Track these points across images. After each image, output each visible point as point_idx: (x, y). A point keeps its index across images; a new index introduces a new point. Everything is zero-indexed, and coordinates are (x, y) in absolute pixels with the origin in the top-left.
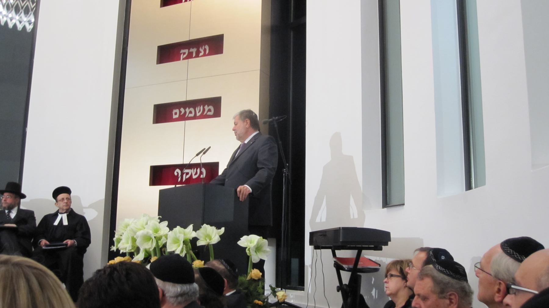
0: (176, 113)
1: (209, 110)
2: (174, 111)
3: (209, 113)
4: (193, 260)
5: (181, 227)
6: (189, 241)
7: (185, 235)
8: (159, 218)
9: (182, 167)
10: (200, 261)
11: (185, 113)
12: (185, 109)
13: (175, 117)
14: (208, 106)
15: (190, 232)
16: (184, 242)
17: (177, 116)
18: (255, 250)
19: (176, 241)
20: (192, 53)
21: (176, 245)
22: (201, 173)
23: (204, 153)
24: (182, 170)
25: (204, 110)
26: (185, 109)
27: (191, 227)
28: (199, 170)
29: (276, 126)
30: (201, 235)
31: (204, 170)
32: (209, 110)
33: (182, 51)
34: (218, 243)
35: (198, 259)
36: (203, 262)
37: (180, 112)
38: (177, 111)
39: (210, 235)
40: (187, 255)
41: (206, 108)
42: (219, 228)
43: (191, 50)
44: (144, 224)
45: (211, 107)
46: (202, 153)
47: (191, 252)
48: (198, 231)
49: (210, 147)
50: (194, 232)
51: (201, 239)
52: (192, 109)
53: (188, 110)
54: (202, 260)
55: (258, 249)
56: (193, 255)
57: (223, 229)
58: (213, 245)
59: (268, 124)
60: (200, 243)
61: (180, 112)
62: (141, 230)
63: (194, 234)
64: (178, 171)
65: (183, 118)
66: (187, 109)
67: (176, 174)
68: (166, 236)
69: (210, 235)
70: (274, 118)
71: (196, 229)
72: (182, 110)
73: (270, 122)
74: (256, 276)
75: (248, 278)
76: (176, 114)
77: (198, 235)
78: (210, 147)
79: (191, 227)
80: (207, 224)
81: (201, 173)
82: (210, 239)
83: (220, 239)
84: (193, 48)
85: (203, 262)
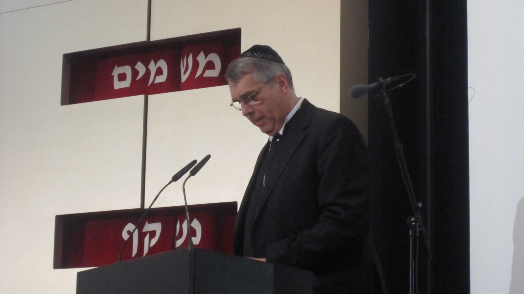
0: (122, 75)
1: (210, 65)
2: (117, 71)
3: (209, 73)
9: (140, 216)
12: (146, 64)
13: (118, 85)
14: (206, 56)
17: (126, 84)
22: (192, 232)
23: (193, 173)
24: (140, 227)
25: (196, 65)
26: (146, 64)
28: (185, 226)
29: (387, 101)
31: (196, 224)
32: (210, 65)
37: (135, 73)
38: (127, 70)
41: (202, 59)
45: (214, 58)
46: (188, 173)
49: (208, 157)
52: (163, 64)
59: (364, 99)
61: (135, 73)
64: (130, 227)
65: (142, 87)
67: (125, 236)
70: (381, 79)
72: (140, 67)
73: (372, 92)
76: (122, 77)
78: (208, 157)
81: (192, 232)
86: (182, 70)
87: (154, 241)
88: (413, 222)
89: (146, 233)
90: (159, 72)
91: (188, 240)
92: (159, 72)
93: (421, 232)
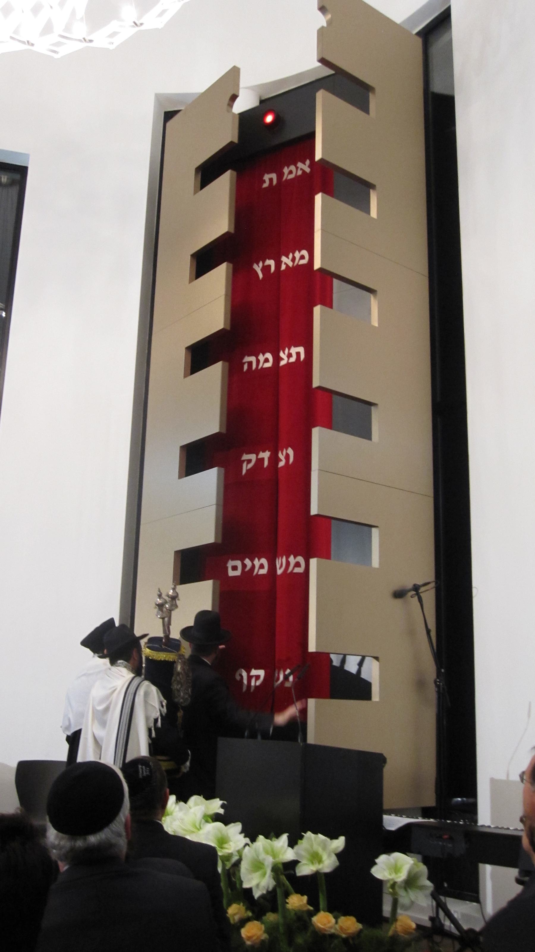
4: (287, 895)
5: (267, 837)
6: (281, 866)
7: (274, 856)
8: (223, 806)
11: (253, 566)
12: (252, 560)
15: (281, 849)
16: (275, 869)
18: (403, 885)
19: (258, 866)
20: (263, 459)
21: (257, 875)
26: (252, 560)
27: (284, 838)
30: (303, 853)
33: (245, 457)
34: (336, 872)
35: (297, 892)
36: (305, 898)
37: (244, 566)
38: (238, 563)
39: (320, 853)
40: (278, 890)
41: (292, 559)
42: (333, 836)
43: (261, 455)
44: (198, 827)
47: (283, 878)
48: (296, 847)
50: (290, 849)
51: (304, 862)
53: (257, 562)
54: (302, 895)
55: (410, 882)
56: (287, 883)
57: (342, 839)
58: (326, 874)
61: (244, 566)
62: (193, 832)
63: (289, 855)
66: (256, 559)
67: (238, 678)
68: (240, 852)
69: (320, 853)
71: (292, 843)
72: (248, 562)
75: (391, 933)
77: (297, 854)
79: (284, 838)
82: (320, 861)
83: (337, 863)
84: (264, 451)
85: (305, 898)
86: (278, 566)
87: (258, 683)
88: (438, 682)
89: (252, 676)
90: (262, 566)
91: (283, 683)
92: (262, 566)
93: (443, 689)
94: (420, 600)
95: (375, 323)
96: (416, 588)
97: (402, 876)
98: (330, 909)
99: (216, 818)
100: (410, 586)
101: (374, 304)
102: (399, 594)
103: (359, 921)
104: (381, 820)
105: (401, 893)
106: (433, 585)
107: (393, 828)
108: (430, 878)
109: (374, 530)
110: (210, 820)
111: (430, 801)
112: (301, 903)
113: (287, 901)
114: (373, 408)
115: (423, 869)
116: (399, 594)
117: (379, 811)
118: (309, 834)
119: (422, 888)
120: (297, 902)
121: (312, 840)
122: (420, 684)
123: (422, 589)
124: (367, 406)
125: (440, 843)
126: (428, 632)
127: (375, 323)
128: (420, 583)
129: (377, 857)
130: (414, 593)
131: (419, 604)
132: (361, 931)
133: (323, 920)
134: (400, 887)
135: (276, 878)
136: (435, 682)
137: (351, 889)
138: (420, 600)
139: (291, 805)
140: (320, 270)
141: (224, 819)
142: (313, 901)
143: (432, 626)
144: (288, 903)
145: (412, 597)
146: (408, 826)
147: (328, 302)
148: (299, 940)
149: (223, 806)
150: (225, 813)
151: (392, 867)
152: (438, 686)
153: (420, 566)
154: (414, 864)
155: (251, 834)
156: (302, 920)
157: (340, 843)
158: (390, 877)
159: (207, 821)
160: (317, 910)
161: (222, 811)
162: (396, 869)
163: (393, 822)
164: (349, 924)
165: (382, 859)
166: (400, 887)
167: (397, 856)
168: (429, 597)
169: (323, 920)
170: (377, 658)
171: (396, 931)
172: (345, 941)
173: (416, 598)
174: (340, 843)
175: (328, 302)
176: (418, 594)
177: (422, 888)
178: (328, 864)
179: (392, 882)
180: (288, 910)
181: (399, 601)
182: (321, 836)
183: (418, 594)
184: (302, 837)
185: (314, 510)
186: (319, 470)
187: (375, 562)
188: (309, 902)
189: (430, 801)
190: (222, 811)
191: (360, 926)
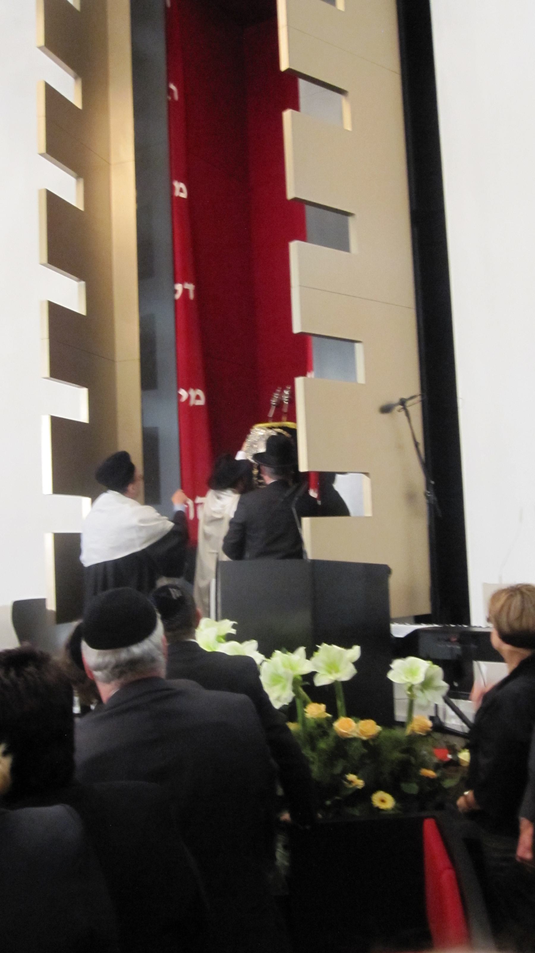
4: (305, 704)
6: (300, 678)
8: (234, 627)
10: (316, 705)
18: (419, 687)
27: (301, 650)
30: (321, 665)
36: (323, 707)
39: (336, 664)
42: (348, 646)
47: (301, 690)
48: (313, 659)
50: (307, 660)
51: (321, 672)
55: (426, 684)
58: (344, 683)
60: (321, 681)
69: (336, 664)
71: (309, 655)
74: (422, 729)
77: (315, 665)
79: (301, 650)
80: (330, 643)
85: (323, 707)
94: (407, 414)
95: (348, 126)
96: (403, 402)
97: (419, 679)
98: (349, 715)
99: (229, 638)
100: (396, 400)
101: (346, 105)
102: (386, 409)
103: (378, 724)
104: (388, 629)
105: (418, 693)
106: (419, 398)
107: (401, 635)
108: (446, 679)
109: (357, 345)
110: (222, 640)
111: (425, 608)
112: (320, 712)
113: (305, 710)
114: (350, 219)
115: (438, 670)
116: (386, 409)
117: (386, 621)
118: (325, 645)
119: (437, 688)
120: (315, 711)
121: (327, 651)
122: (410, 497)
123: (408, 403)
124: (344, 217)
125: (449, 646)
126: (416, 445)
127: (348, 126)
128: (405, 396)
129: (391, 662)
130: (401, 407)
131: (405, 418)
132: (380, 733)
133: (345, 726)
134: (417, 689)
135: (295, 690)
136: (425, 494)
137: (369, 694)
138: (407, 414)
139: (301, 620)
140: (289, 71)
141: (240, 637)
142: (332, 709)
143: (420, 439)
144: (306, 712)
145: (399, 411)
146: (415, 633)
147: (296, 106)
148: (322, 745)
149: (234, 627)
150: (237, 632)
151: (408, 672)
152: (428, 498)
153: (405, 379)
154: (430, 667)
155: (267, 651)
156: (323, 728)
157: (355, 652)
158: (407, 680)
159: (220, 642)
160: (336, 717)
161: (233, 631)
162: (412, 672)
163: (400, 630)
164: (368, 728)
165: (397, 664)
166: (417, 689)
167: (412, 660)
168: (416, 410)
169: (345, 726)
170: (366, 474)
171: (413, 731)
172: (365, 743)
173: (403, 413)
174: (355, 652)
175: (296, 106)
176: (405, 408)
177: (437, 688)
178: (346, 672)
179: (409, 685)
180: (307, 718)
181: (386, 416)
182: (335, 647)
183: (405, 408)
184: (317, 650)
185: (297, 329)
186: (300, 286)
187: (361, 378)
188: (328, 711)
189: (425, 608)
190: (233, 631)
191: (379, 728)
